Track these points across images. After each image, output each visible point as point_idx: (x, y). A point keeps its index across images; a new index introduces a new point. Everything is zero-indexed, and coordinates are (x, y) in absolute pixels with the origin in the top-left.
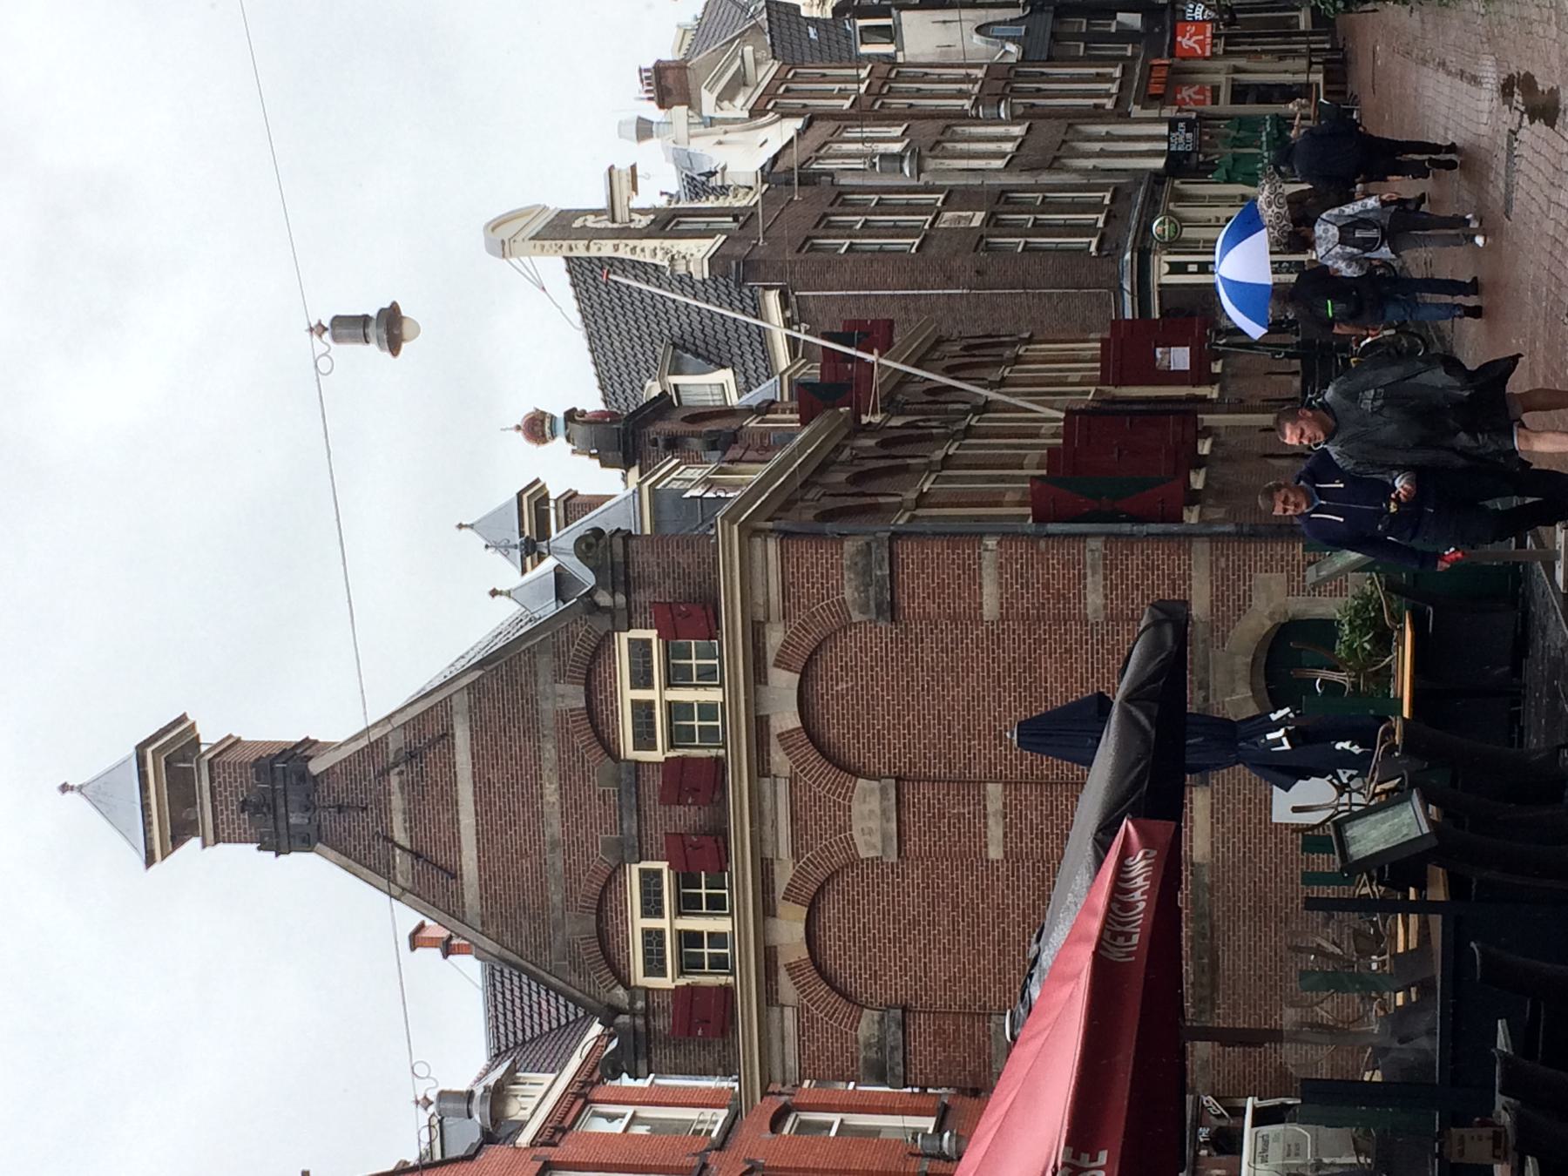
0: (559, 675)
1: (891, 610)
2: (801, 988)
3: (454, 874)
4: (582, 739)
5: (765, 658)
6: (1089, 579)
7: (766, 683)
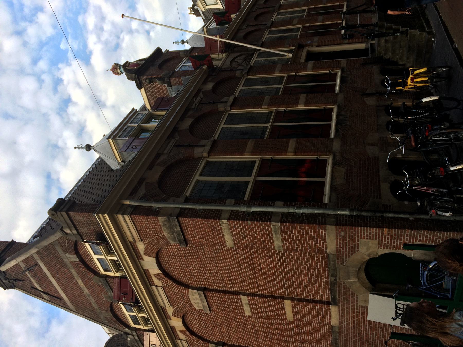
0: (66, 252)
1: (186, 242)
2: (186, 336)
3: (61, 299)
4: (84, 269)
6: (274, 236)
7: (143, 260)
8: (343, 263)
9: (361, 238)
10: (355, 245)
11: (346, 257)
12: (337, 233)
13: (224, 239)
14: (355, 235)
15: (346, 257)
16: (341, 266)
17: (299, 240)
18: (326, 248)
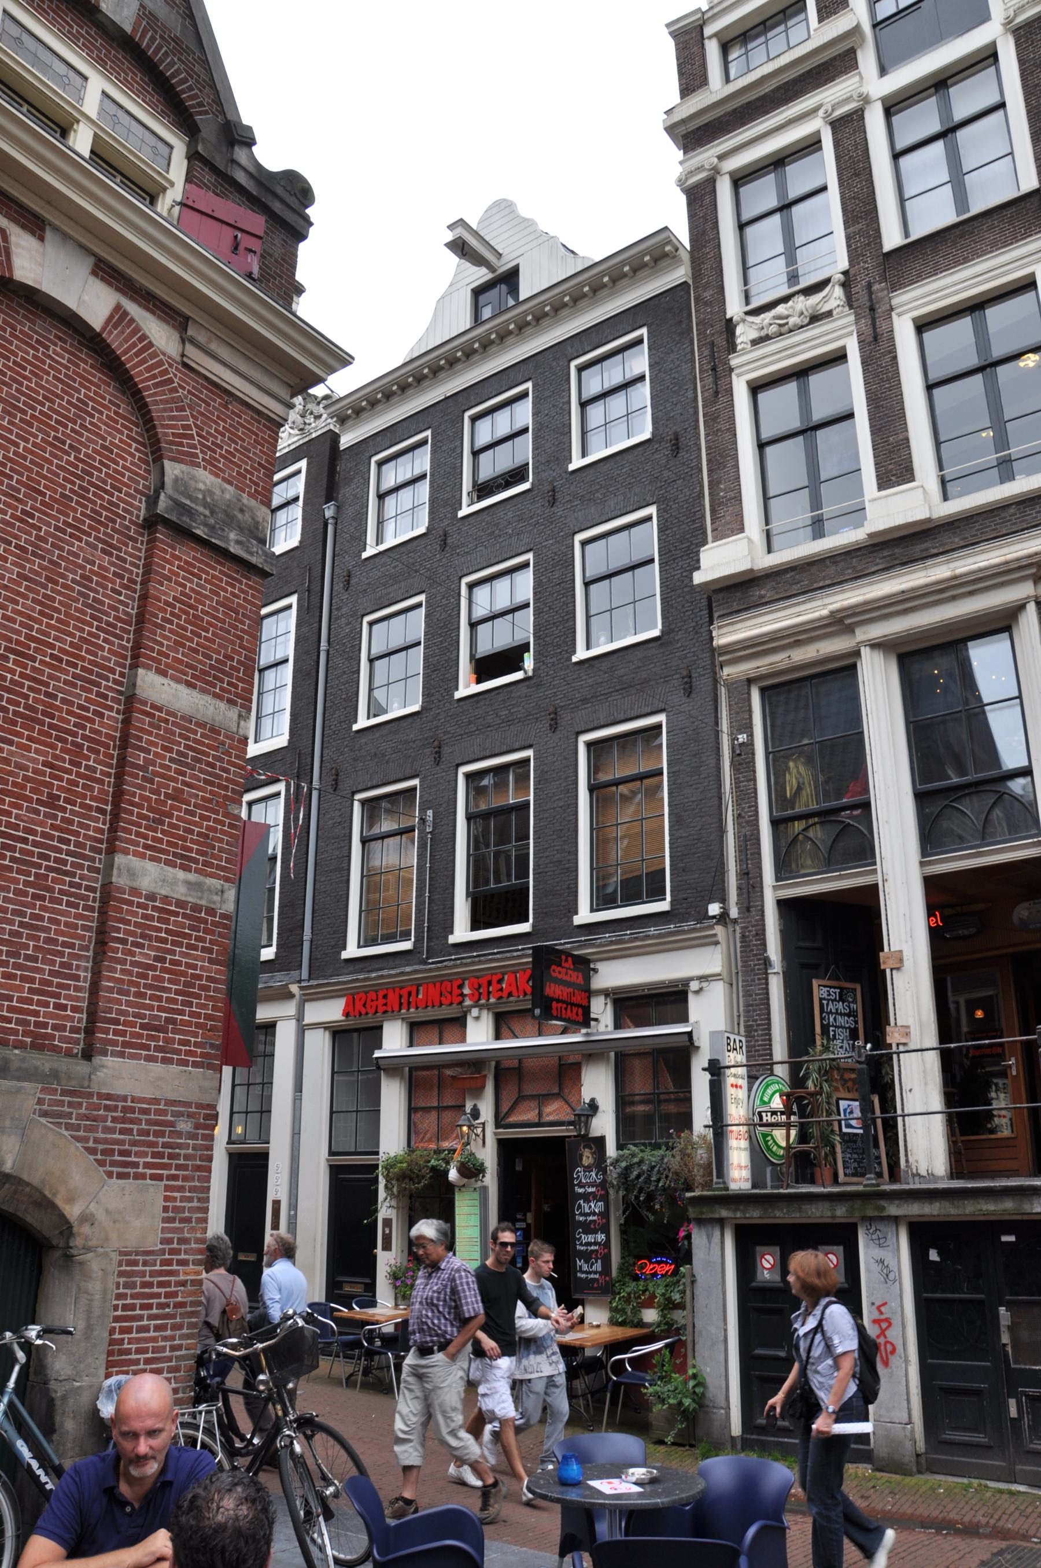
5: (132, 299)
6: (181, 875)
8: (45, 1114)
9: (167, 1188)
10: (135, 1165)
11: (77, 1128)
12: (188, 1104)
13: (178, 681)
14: (179, 1167)
15: (77, 1128)
16: (31, 1103)
17: (157, 959)
18: (121, 1055)
